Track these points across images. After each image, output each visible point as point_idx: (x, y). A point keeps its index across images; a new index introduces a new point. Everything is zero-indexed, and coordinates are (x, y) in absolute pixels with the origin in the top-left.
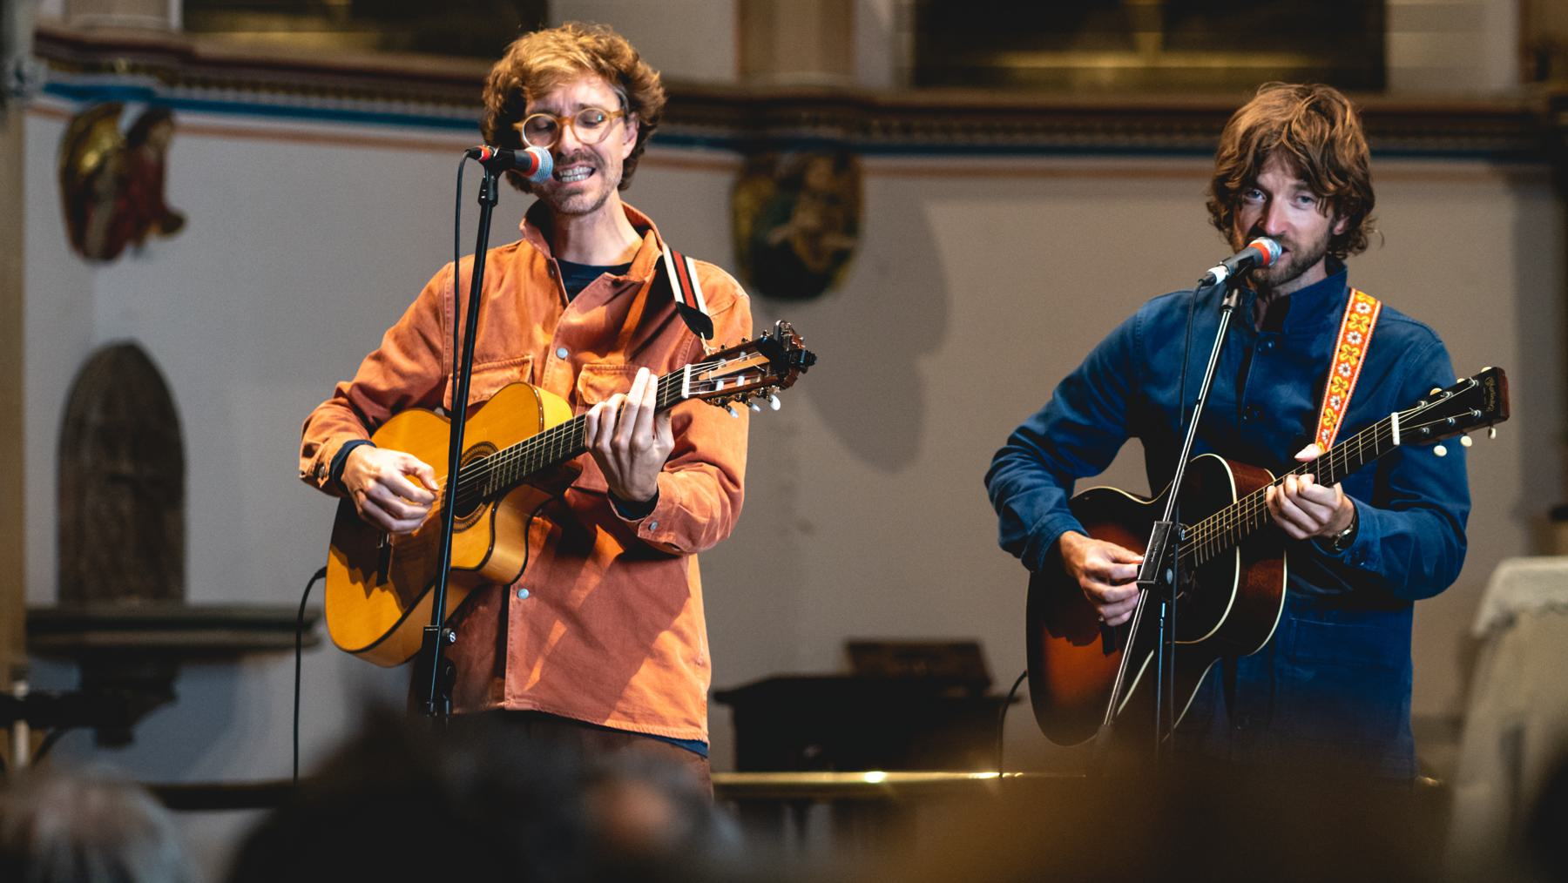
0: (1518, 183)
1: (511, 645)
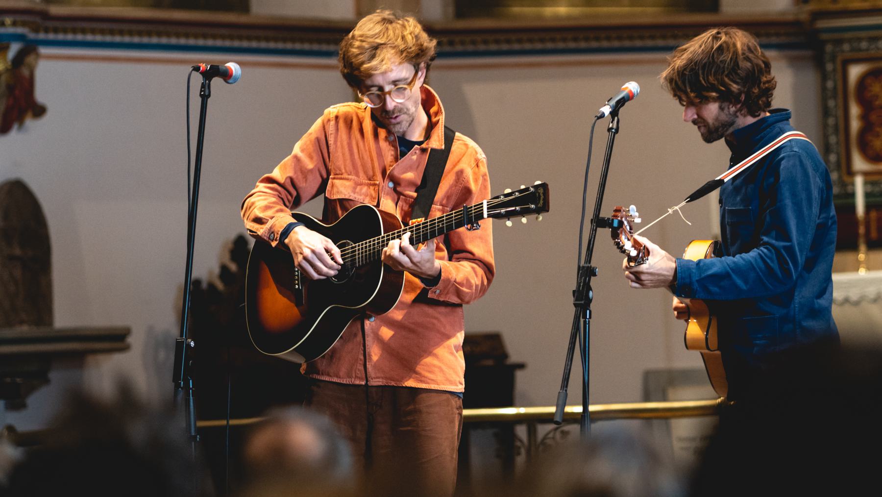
1: (368, 348)
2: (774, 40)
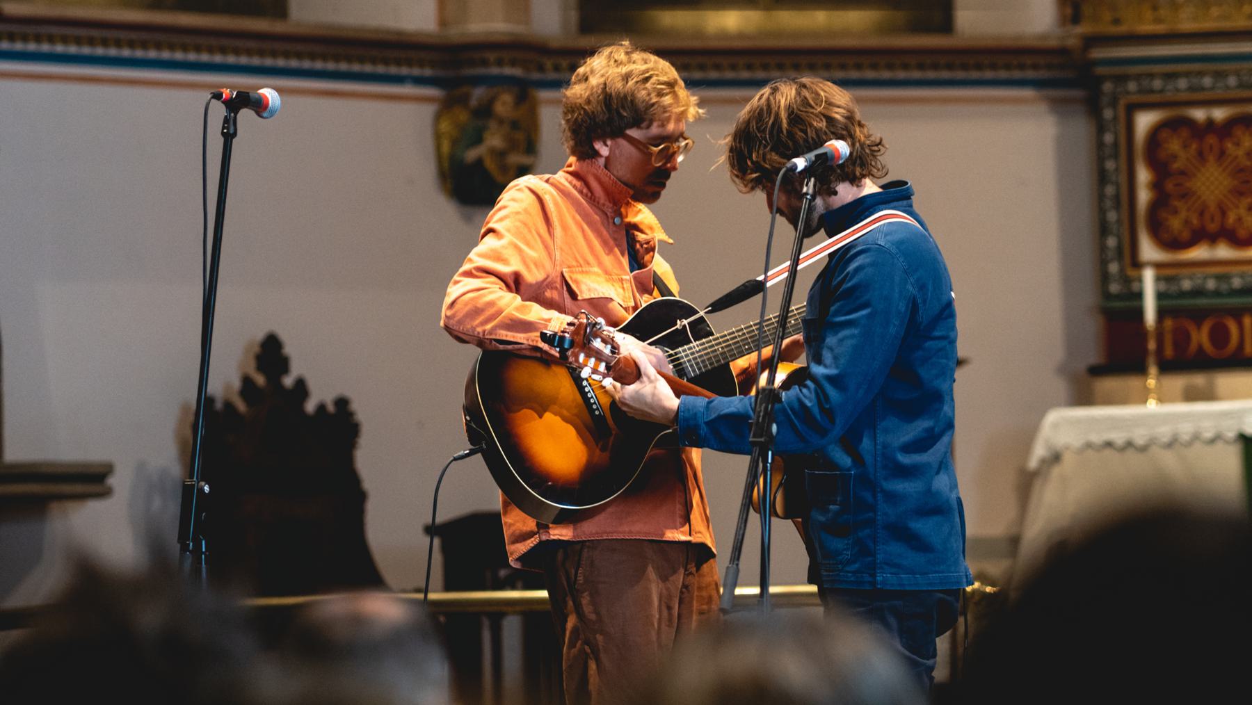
0: (1058, 106)
2: (1030, 74)
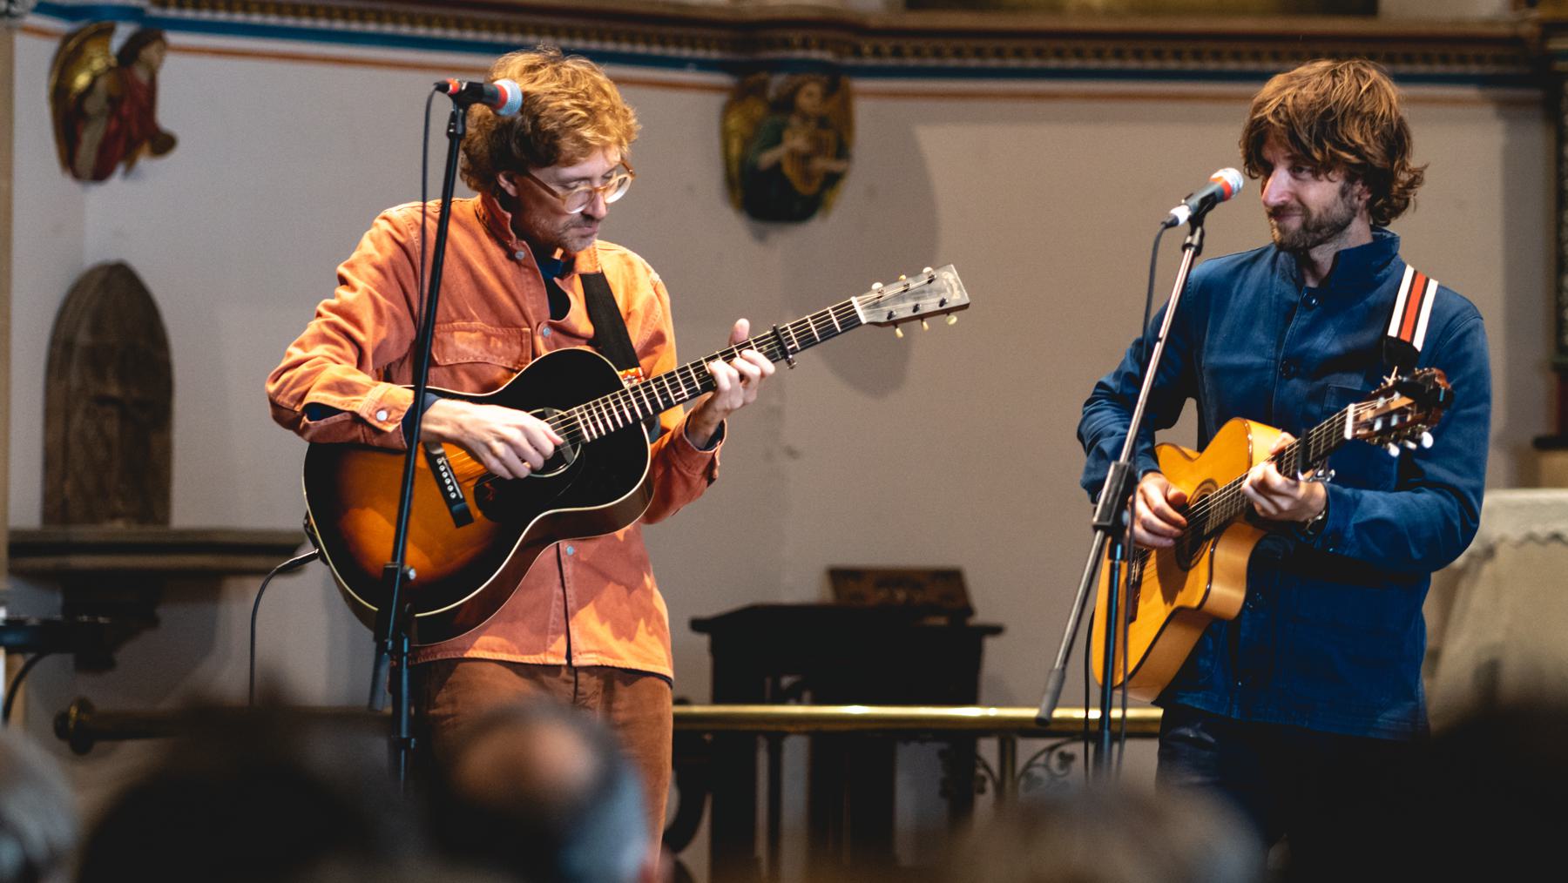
0: (1506, 108)
2: (1474, 69)
